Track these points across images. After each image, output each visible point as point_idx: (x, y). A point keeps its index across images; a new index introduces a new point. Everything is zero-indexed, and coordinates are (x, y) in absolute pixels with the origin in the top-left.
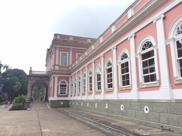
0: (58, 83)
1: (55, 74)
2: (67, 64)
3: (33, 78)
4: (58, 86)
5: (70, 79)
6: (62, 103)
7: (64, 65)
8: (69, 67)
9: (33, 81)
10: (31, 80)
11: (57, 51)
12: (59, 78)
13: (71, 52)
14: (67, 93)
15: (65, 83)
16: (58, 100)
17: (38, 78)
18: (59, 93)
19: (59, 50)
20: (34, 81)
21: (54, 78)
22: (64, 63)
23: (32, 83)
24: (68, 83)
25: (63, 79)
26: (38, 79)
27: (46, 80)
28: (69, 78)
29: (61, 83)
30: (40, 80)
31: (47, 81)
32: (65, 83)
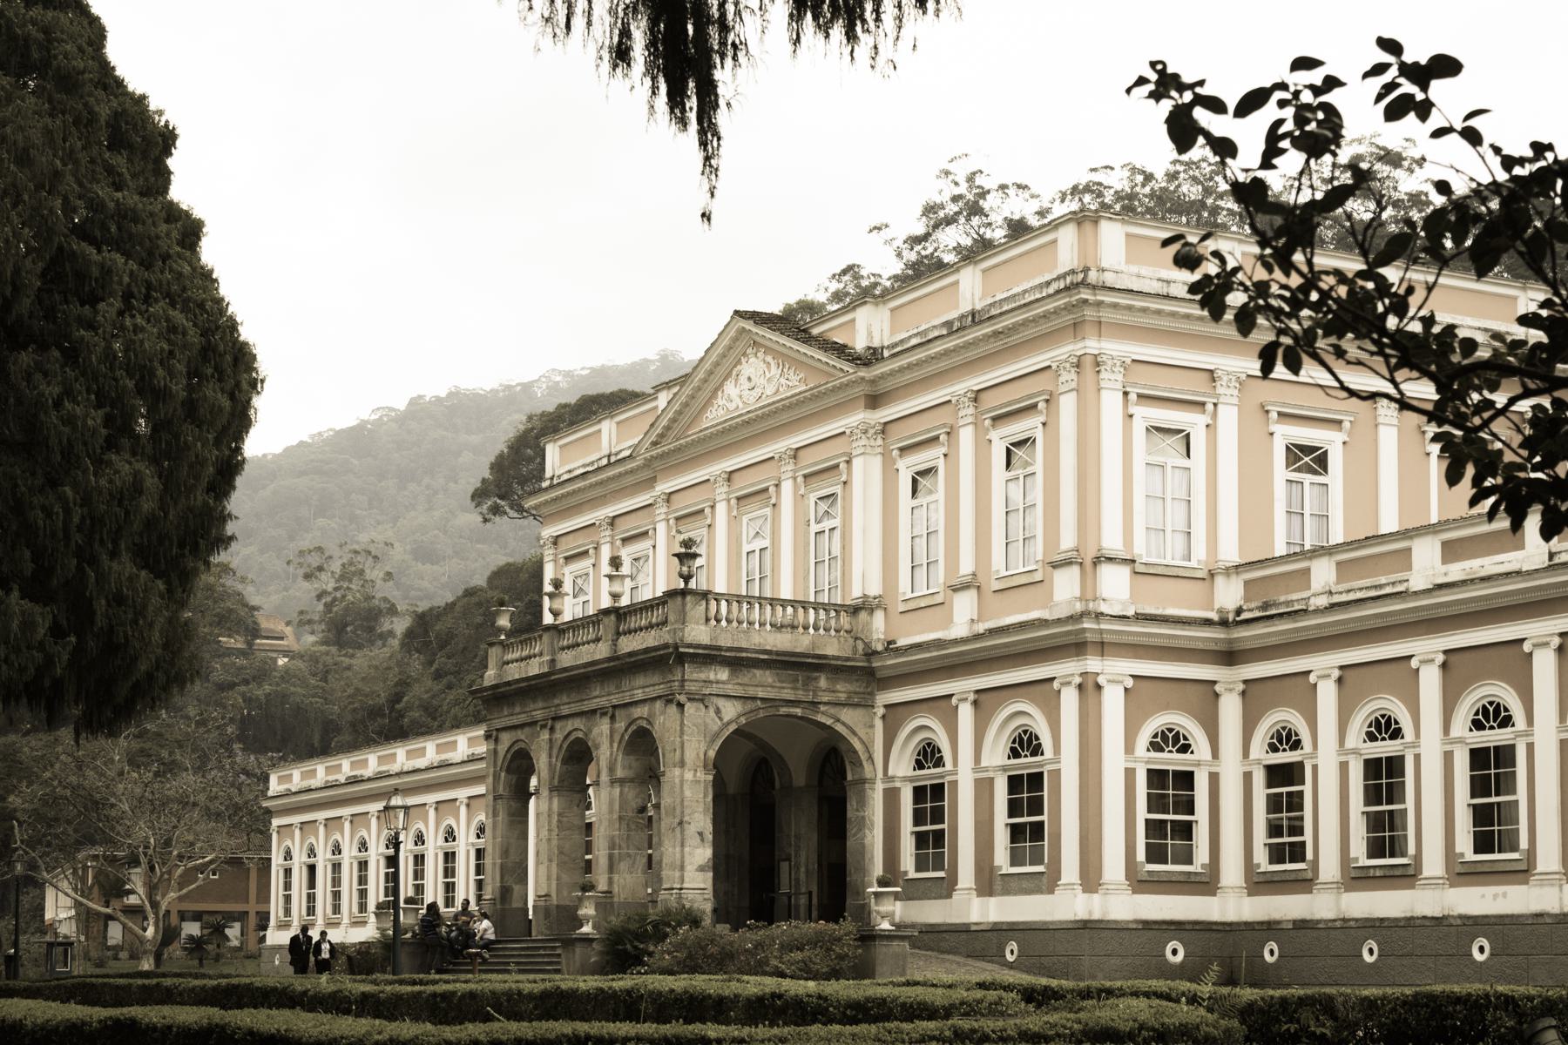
0: (1129, 748)
1: (1103, 648)
2: (1200, 554)
3: (723, 674)
4: (1130, 774)
5: (1230, 710)
6: (1175, 952)
7: (1168, 561)
8: (1220, 581)
9: (718, 711)
10: (702, 699)
11: (1111, 402)
12: (1141, 693)
13: (1228, 417)
14: (1202, 855)
15: (1185, 749)
16: (1147, 925)
17: (767, 676)
18: (1141, 855)
19: (1126, 394)
20: (730, 710)
21: (1089, 688)
22: (1169, 530)
23: (717, 735)
24: (1215, 754)
25: (1167, 707)
26: (765, 684)
27: (843, 697)
28: (1217, 695)
29: (1155, 746)
30: (788, 694)
31: (847, 715)
32: (1185, 749)
